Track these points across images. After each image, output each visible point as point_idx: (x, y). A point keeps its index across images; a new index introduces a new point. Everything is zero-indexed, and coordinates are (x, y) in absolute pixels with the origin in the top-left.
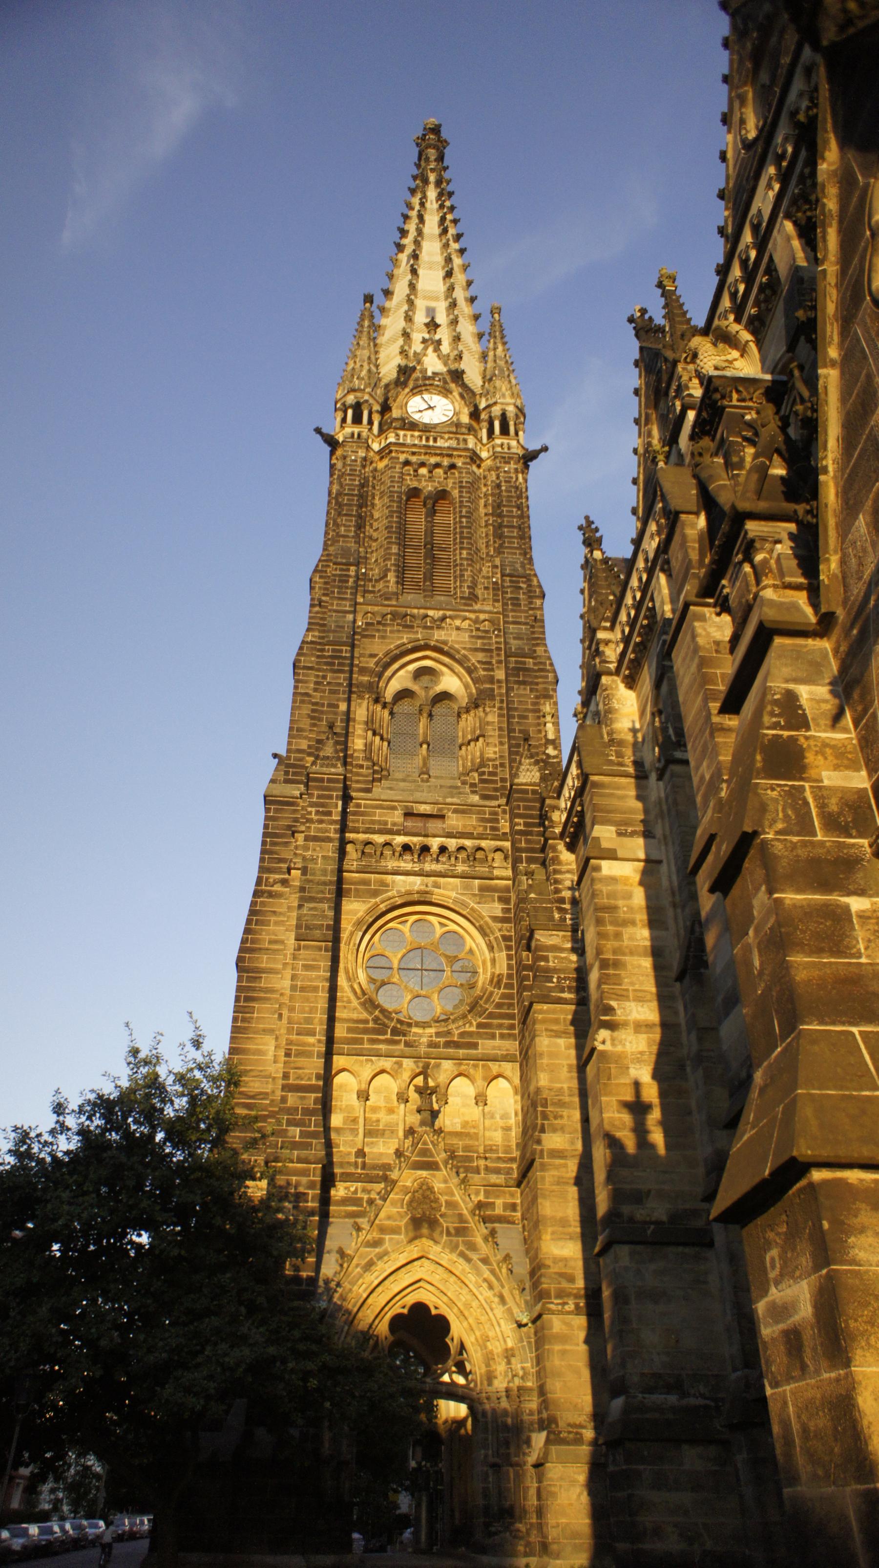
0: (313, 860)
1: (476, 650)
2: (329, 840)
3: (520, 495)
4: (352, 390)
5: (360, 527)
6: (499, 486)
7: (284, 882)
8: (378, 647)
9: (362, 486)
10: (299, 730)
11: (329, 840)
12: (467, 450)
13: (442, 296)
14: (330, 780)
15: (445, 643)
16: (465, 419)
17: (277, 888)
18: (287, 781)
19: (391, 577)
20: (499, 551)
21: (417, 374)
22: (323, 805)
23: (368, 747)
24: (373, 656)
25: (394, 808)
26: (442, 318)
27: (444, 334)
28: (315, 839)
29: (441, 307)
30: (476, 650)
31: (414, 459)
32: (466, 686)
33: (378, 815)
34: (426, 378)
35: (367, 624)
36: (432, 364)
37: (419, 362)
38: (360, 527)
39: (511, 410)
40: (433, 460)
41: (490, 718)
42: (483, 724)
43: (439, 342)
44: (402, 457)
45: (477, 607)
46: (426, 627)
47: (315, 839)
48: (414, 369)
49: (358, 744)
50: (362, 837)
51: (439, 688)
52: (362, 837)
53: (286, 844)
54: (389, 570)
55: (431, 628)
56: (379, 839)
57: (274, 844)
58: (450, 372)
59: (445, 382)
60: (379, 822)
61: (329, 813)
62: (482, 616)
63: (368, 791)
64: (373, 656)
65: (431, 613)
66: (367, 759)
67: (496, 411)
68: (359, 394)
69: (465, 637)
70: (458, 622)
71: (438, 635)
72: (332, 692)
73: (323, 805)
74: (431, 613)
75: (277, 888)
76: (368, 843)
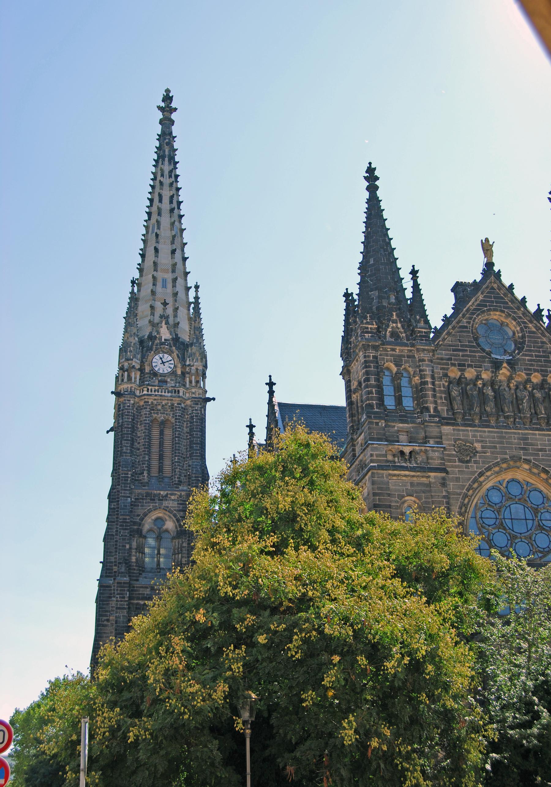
0: (119, 617)
1: (180, 511)
2: (124, 608)
3: (202, 420)
4: (127, 360)
5: (132, 444)
6: (192, 418)
7: (108, 620)
8: (140, 511)
9: (133, 420)
10: (111, 552)
11: (124, 608)
12: (179, 397)
13: (170, 270)
14: (124, 583)
15: (168, 507)
16: (179, 372)
17: (105, 623)
18: (107, 576)
19: (145, 474)
20: (191, 455)
21: (157, 341)
22: (122, 594)
23: (137, 559)
24: (138, 515)
25: (147, 588)
26: (170, 300)
27: (170, 311)
28: (119, 608)
29: (170, 300)
30: (180, 511)
31: (155, 402)
32: (176, 528)
33: (141, 591)
34: (162, 344)
35: (136, 499)
36: (165, 334)
37: (158, 333)
38: (132, 445)
39: (201, 368)
40: (164, 403)
41: (184, 545)
42: (182, 547)
43: (168, 317)
44: (150, 401)
45: (181, 488)
46: (159, 500)
47: (119, 608)
48: (156, 337)
49: (134, 559)
50: (136, 602)
51: (165, 527)
52: (136, 602)
53: (108, 604)
54: (144, 470)
55: (162, 500)
56: (142, 602)
57: (103, 604)
58: (173, 339)
59: (171, 347)
60: (142, 594)
61: (124, 598)
62: (183, 493)
63: (137, 580)
64: (138, 515)
65: (162, 493)
66: (136, 566)
67: (193, 371)
68: (130, 362)
69: (175, 504)
70: (173, 497)
71: (165, 504)
72: (124, 539)
73: (122, 594)
74: (162, 493)
75: (105, 623)
76: (138, 604)
